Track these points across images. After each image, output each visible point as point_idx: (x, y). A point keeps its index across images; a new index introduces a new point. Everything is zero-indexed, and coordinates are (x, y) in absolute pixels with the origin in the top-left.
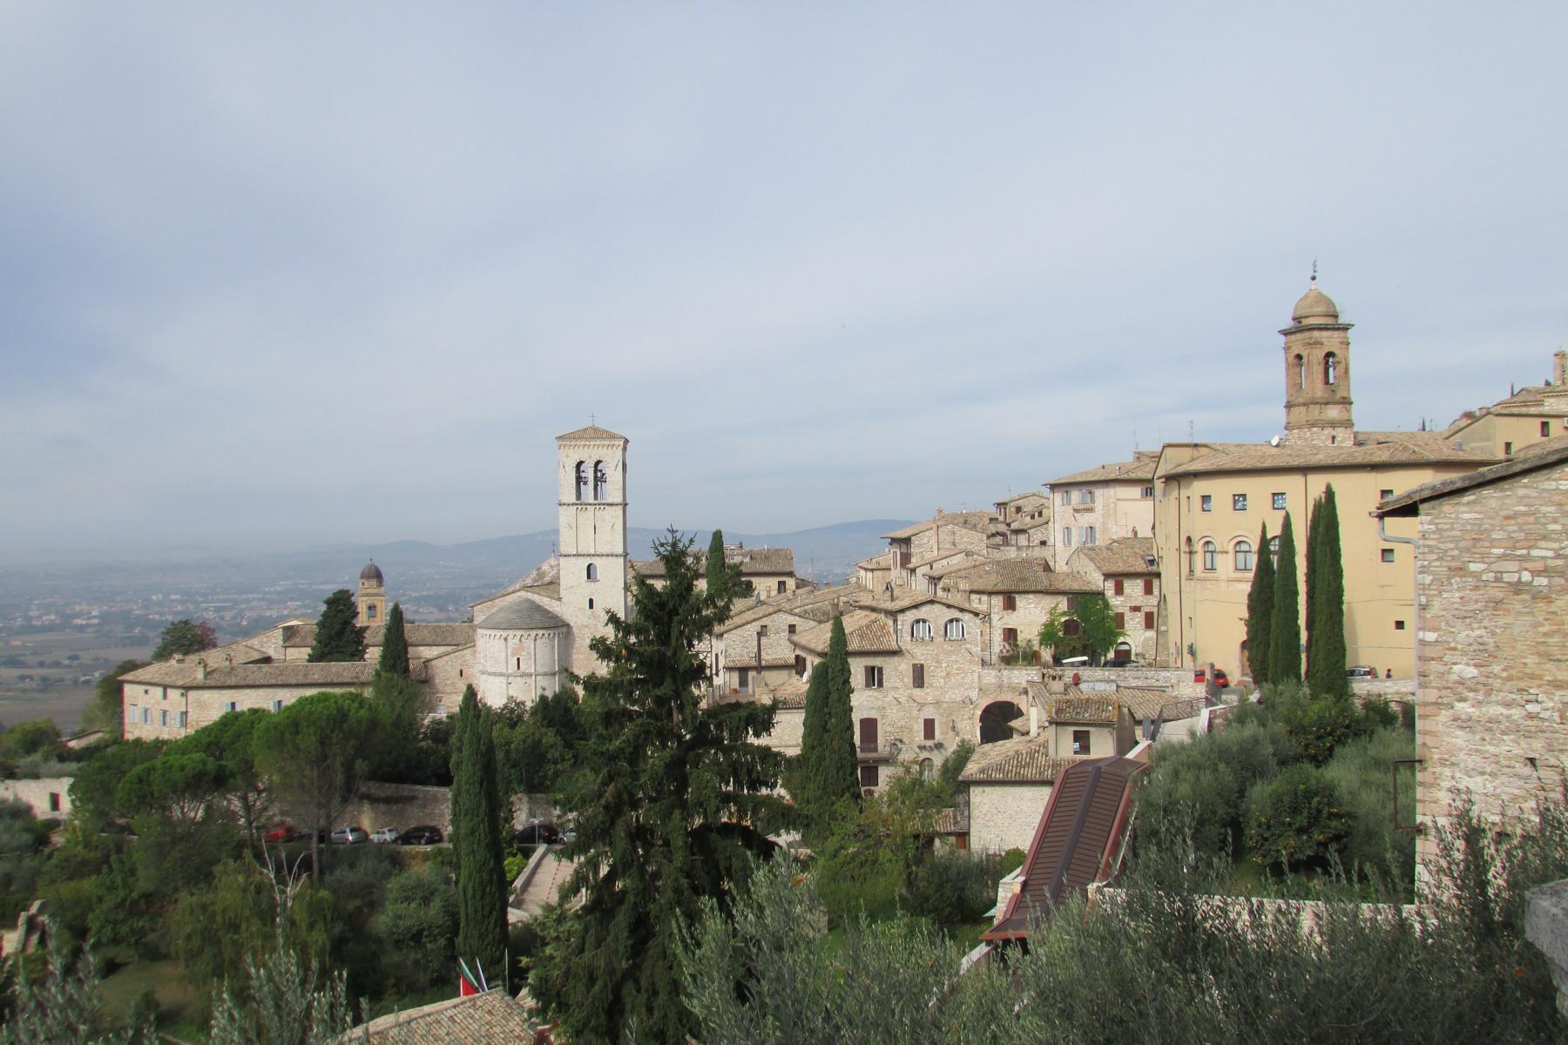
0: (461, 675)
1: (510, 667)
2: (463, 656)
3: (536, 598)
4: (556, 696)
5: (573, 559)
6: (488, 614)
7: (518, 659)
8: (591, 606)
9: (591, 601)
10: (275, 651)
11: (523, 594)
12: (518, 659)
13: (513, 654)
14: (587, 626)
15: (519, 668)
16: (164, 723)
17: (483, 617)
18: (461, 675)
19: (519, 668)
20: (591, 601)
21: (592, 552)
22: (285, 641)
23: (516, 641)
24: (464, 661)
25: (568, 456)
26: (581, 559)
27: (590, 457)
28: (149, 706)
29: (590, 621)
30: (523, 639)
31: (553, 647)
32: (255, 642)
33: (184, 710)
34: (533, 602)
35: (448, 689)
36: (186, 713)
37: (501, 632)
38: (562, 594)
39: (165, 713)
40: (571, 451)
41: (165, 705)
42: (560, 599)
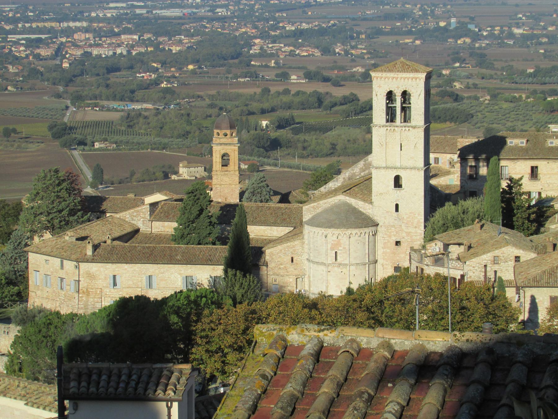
0: (292, 261)
1: (329, 259)
2: (294, 247)
3: (353, 201)
4: (361, 288)
5: (383, 171)
6: (314, 214)
7: (336, 252)
8: (397, 209)
9: (397, 206)
10: (143, 224)
11: (341, 198)
12: (336, 252)
13: (332, 249)
15: (336, 259)
16: (62, 289)
17: (310, 216)
18: (292, 261)
19: (336, 259)
20: (397, 206)
21: (398, 165)
22: (151, 215)
23: (335, 238)
24: (294, 251)
25: (380, 87)
26: (390, 171)
27: (398, 88)
28: (49, 273)
29: (396, 222)
30: (339, 237)
31: (364, 244)
32: (126, 215)
33: (78, 279)
34: (349, 206)
36: (79, 281)
38: (374, 198)
39: (62, 279)
41: (62, 274)
42: (371, 203)
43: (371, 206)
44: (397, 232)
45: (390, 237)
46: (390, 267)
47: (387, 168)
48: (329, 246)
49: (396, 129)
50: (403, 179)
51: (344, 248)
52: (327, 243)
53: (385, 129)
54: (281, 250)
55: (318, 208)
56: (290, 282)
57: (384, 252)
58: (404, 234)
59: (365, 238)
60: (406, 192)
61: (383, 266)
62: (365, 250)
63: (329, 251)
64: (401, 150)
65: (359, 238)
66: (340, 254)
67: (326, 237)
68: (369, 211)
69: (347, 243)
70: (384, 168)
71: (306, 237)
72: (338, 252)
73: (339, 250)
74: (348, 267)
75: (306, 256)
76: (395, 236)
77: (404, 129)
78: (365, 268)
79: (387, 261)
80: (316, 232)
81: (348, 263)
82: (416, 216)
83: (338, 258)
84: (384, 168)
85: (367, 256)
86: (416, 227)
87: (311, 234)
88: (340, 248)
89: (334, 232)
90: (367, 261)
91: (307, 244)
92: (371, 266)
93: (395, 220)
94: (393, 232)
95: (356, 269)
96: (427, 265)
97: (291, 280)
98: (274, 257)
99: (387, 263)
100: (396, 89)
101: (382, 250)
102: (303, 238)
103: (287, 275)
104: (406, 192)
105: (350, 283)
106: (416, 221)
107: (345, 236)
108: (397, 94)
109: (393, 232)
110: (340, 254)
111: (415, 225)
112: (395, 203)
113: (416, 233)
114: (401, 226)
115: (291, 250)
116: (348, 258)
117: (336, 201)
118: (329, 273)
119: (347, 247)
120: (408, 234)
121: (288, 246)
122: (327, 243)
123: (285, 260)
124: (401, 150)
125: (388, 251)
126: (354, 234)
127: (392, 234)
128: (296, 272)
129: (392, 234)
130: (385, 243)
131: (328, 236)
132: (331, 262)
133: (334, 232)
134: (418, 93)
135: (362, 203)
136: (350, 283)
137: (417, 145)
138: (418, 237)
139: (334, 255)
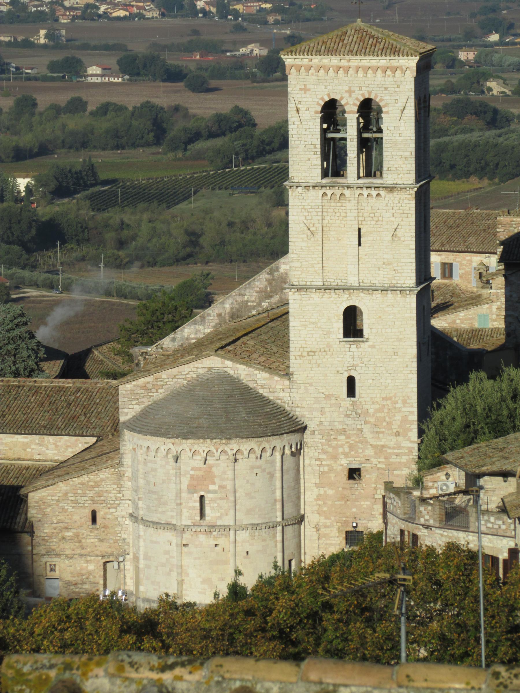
1: (185, 513)
2: (97, 484)
5: (315, 297)
6: (146, 402)
7: (202, 497)
8: (351, 391)
9: (351, 382)
12: (202, 497)
13: (192, 489)
14: (342, 432)
17: (138, 409)
20: (351, 382)
21: (353, 281)
23: (198, 461)
24: (99, 494)
25: (305, 90)
27: (350, 92)
29: (349, 421)
30: (211, 461)
31: (272, 476)
35: (68, 548)
37: (171, 446)
38: (294, 363)
40: (312, 79)
42: (288, 375)
43: (287, 382)
44: (351, 447)
45: (335, 457)
46: (334, 532)
47: (325, 288)
48: (185, 482)
49: (347, 192)
50: (365, 317)
51: (222, 487)
52: (179, 475)
53: (321, 192)
54: (66, 494)
55: (157, 388)
56: (90, 573)
57: (319, 495)
58: (369, 452)
59: (273, 463)
60: (373, 347)
61: (318, 530)
62: (274, 492)
63: (184, 495)
64: (360, 244)
65: (259, 462)
66: (213, 500)
67: (176, 459)
68: (282, 395)
69: (230, 474)
70: (318, 288)
71: (127, 460)
72: (208, 497)
73: (209, 492)
74: (232, 532)
75: (127, 508)
76: (346, 455)
77: (365, 192)
78: (275, 536)
79: (327, 518)
80: (153, 448)
81: (232, 523)
83: (208, 510)
84: (318, 288)
85: (279, 506)
86: (398, 434)
87: (141, 454)
88: (212, 487)
89: (196, 447)
90: (279, 519)
91: (130, 479)
92: (289, 530)
93: (347, 416)
94: (342, 446)
95: (253, 537)
96: (427, 527)
97: (91, 567)
98: (48, 510)
99: (328, 522)
100: (346, 95)
101: (316, 491)
102: (120, 464)
103: (81, 555)
104: (373, 347)
105: (238, 573)
106: (398, 417)
108: (347, 108)
109: (342, 446)
110: (213, 500)
111: (395, 428)
112: (346, 375)
113: (400, 448)
114: (361, 430)
115: (90, 494)
116: (232, 512)
117: (201, 371)
118: (185, 549)
119: (229, 485)
120: (380, 450)
121: (83, 484)
122: (179, 475)
123: (76, 517)
124: (360, 244)
125: (330, 492)
126: (246, 453)
127: (340, 450)
128: (103, 548)
129: (340, 450)
130: (323, 473)
131: (183, 458)
132: (189, 523)
133: (196, 447)
134: (400, 105)
135: (267, 375)
136: (238, 573)
137: (399, 233)
139: (198, 504)
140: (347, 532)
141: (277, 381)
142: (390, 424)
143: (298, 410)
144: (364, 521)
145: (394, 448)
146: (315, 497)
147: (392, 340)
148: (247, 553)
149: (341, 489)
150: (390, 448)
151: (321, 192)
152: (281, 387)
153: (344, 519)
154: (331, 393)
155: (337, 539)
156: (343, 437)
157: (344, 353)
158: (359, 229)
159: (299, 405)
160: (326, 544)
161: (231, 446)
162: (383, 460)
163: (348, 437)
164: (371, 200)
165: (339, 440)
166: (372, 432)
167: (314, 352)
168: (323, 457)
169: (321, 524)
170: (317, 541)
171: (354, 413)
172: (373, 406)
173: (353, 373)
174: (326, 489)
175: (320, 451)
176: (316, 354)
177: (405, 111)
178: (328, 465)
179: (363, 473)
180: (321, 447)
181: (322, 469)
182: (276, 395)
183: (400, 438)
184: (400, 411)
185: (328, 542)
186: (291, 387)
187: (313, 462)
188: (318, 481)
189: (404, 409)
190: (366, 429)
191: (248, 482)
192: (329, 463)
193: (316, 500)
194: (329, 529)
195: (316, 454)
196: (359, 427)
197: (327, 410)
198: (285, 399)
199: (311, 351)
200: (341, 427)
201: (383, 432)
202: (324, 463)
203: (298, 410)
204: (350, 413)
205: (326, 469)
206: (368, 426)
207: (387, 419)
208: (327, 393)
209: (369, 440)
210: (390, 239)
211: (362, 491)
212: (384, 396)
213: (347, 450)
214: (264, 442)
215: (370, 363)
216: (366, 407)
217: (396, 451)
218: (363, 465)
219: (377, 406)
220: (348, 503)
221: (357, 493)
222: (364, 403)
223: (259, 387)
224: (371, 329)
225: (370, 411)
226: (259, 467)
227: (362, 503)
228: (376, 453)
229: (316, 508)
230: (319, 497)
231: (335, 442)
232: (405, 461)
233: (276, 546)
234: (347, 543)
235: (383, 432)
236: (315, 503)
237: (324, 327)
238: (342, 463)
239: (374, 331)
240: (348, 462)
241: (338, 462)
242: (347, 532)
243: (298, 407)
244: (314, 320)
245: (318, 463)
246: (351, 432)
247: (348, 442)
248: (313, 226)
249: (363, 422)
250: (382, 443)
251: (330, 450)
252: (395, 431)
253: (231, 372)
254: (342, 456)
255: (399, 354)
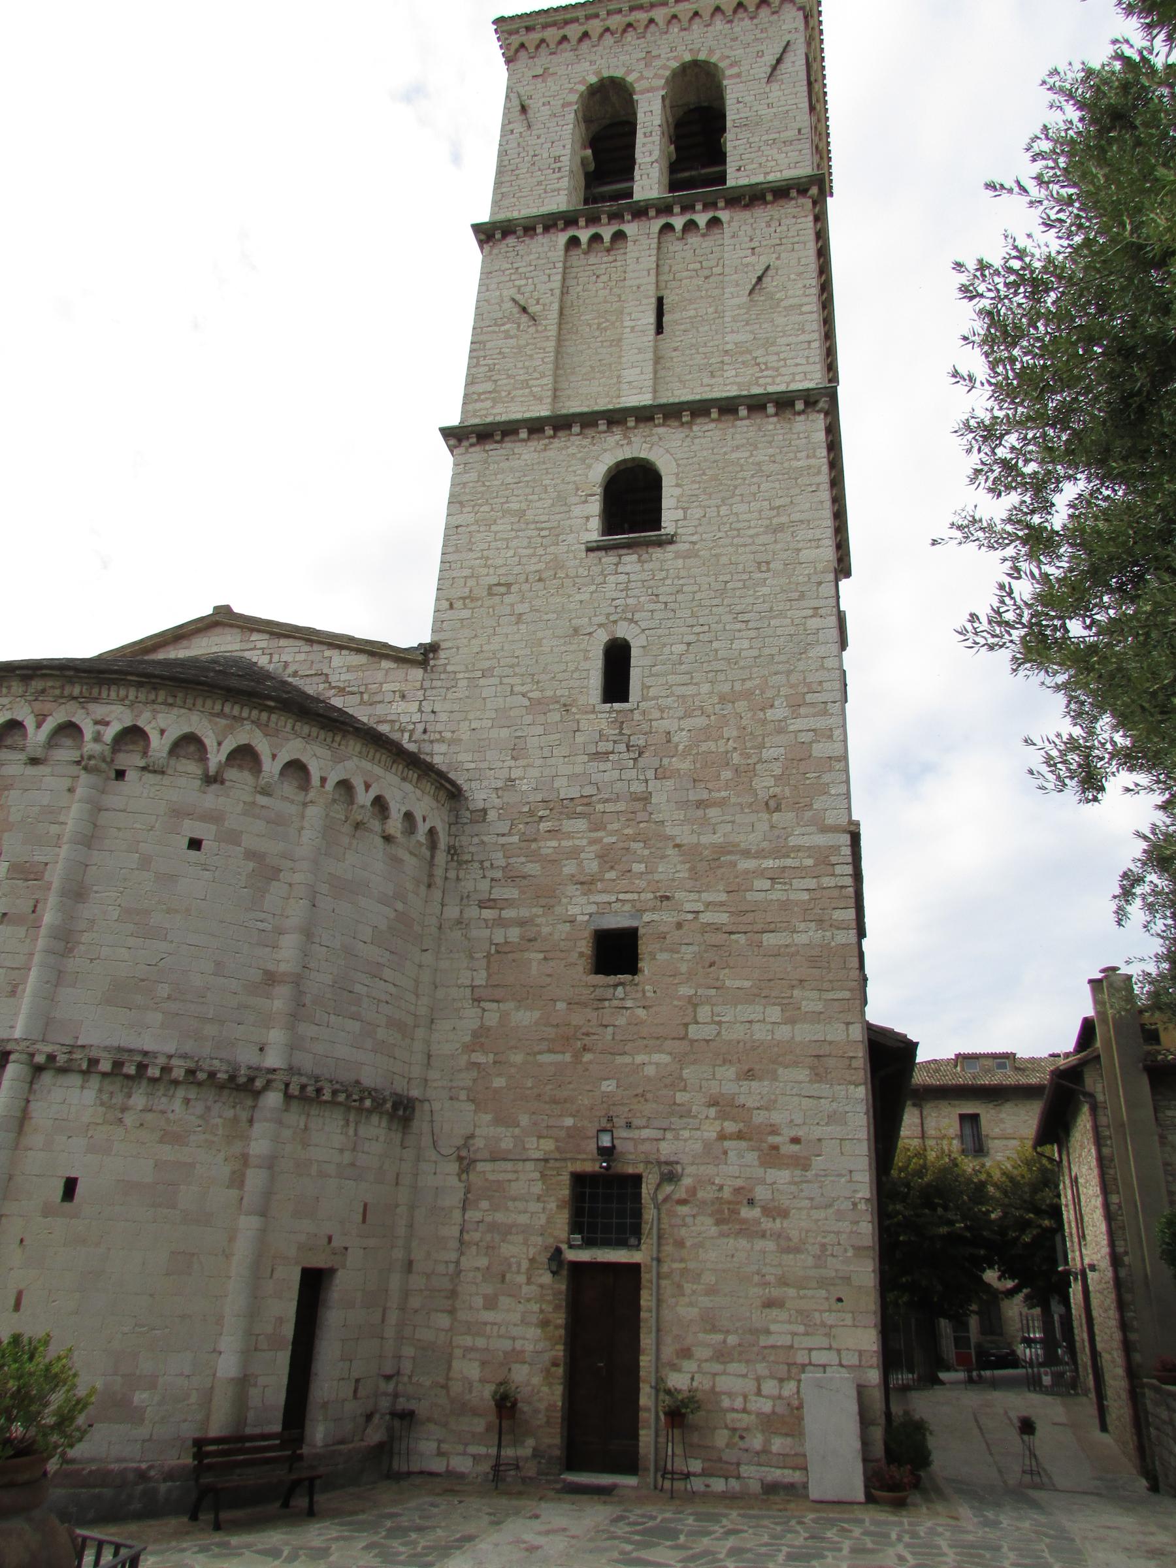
26: (572, 445)
29: (605, 772)
44: (607, 858)
45: (547, 896)
49: (630, 229)
50: (665, 482)
53: (562, 238)
58: (671, 869)
64: (659, 329)
68: (399, 707)
70: (535, 427)
76: (587, 884)
82: (779, 712)
86: (773, 805)
93: (598, 756)
94: (575, 853)
107: (65, 753)
111: (764, 784)
113: (780, 852)
114: (645, 798)
125: (524, 1018)
130: (501, 950)
138: (799, 891)
140: (579, 1180)
141: (387, 671)
142: (745, 773)
143: (440, 748)
144: (646, 1133)
145: (761, 854)
146: (468, 1038)
147: (752, 532)
148: (70, 1187)
149: (561, 1006)
150: (746, 853)
151: (562, 238)
152: (396, 686)
153: (569, 1122)
154: (549, 693)
155: (534, 1206)
156: (581, 824)
157: (600, 579)
158: (660, 301)
159: (448, 735)
160: (493, 1227)
161: (99, 710)
162: (723, 897)
163: (597, 827)
164: (693, 240)
165: (569, 836)
166: (683, 804)
167: (509, 585)
168: (511, 893)
169: (479, 1143)
170: (457, 1214)
171: (622, 747)
172: (687, 723)
173: (623, 631)
174: (509, 1005)
175: (498, 874)
176: (514, 588)
177: (782, 67)
178: (522, 923)
179: (644, 948)
180: (502, 862)
181: (499, 936)
182: (380, 710)
183: (784, 818)
184: (781, 731)
185: (500, 1217)
186: (427, 684)
187: (473, 912)
188: (481, 978)
189: (796, 725)
190: (662, 795)
191: (145, 862)
192: (524, 913)
193: (469, 1048)
194: (509, 1166)
195: (484, 885)
196: (638, 788)
197: (533, 742)
198: (404, 719)
199: (499, 584)
200: (574, 793)
201: (722, 803)
202: (508, 914)
203: (440, 748)
204: (609, 746)
205: (514, 934)
206: (669, 783)
207: (736, 758)
208: (536, 695)
209: (669, 830)
210: (745, 299)
211: (641, 1012)
212: (726, 688)
213: (593, 866)
214: (248, 726)
215: (680, 597)
216: (665, 724)
217: (769, 863)
218: (647, 917)
219: (700, 721)
220: (588, 1057)
221: (621, 1021)
222: (656, 714)
223: (333, 692)
224: (685, 509)
225: (675, 739)
226: (214, 817)
227: (639, 1059)
228: (694, 873)
229: (466, 1079)
230: (480, 1038)
231: (554, 844)
232: (805, 896)
233: (237, 1180)
234: (576, 1226)
235: (722, 803)
236: (463, 1060)
237: (543, 518)
238: (573, 910)
239: (696, 513)
240: (593, 909)
241: (558, 910)
242: (579, 1180)
243: (442, 740)
244: (514, 506)
245: (487, 914)
246: (610, 807)
247: (598, 841)
248: (538, 303)
249: (650, 774)
250: (717, 839)
251: (533, 868)
252: (763, 795)
253: (263, 661)
254: (571, 889)
255: (776, 565)
